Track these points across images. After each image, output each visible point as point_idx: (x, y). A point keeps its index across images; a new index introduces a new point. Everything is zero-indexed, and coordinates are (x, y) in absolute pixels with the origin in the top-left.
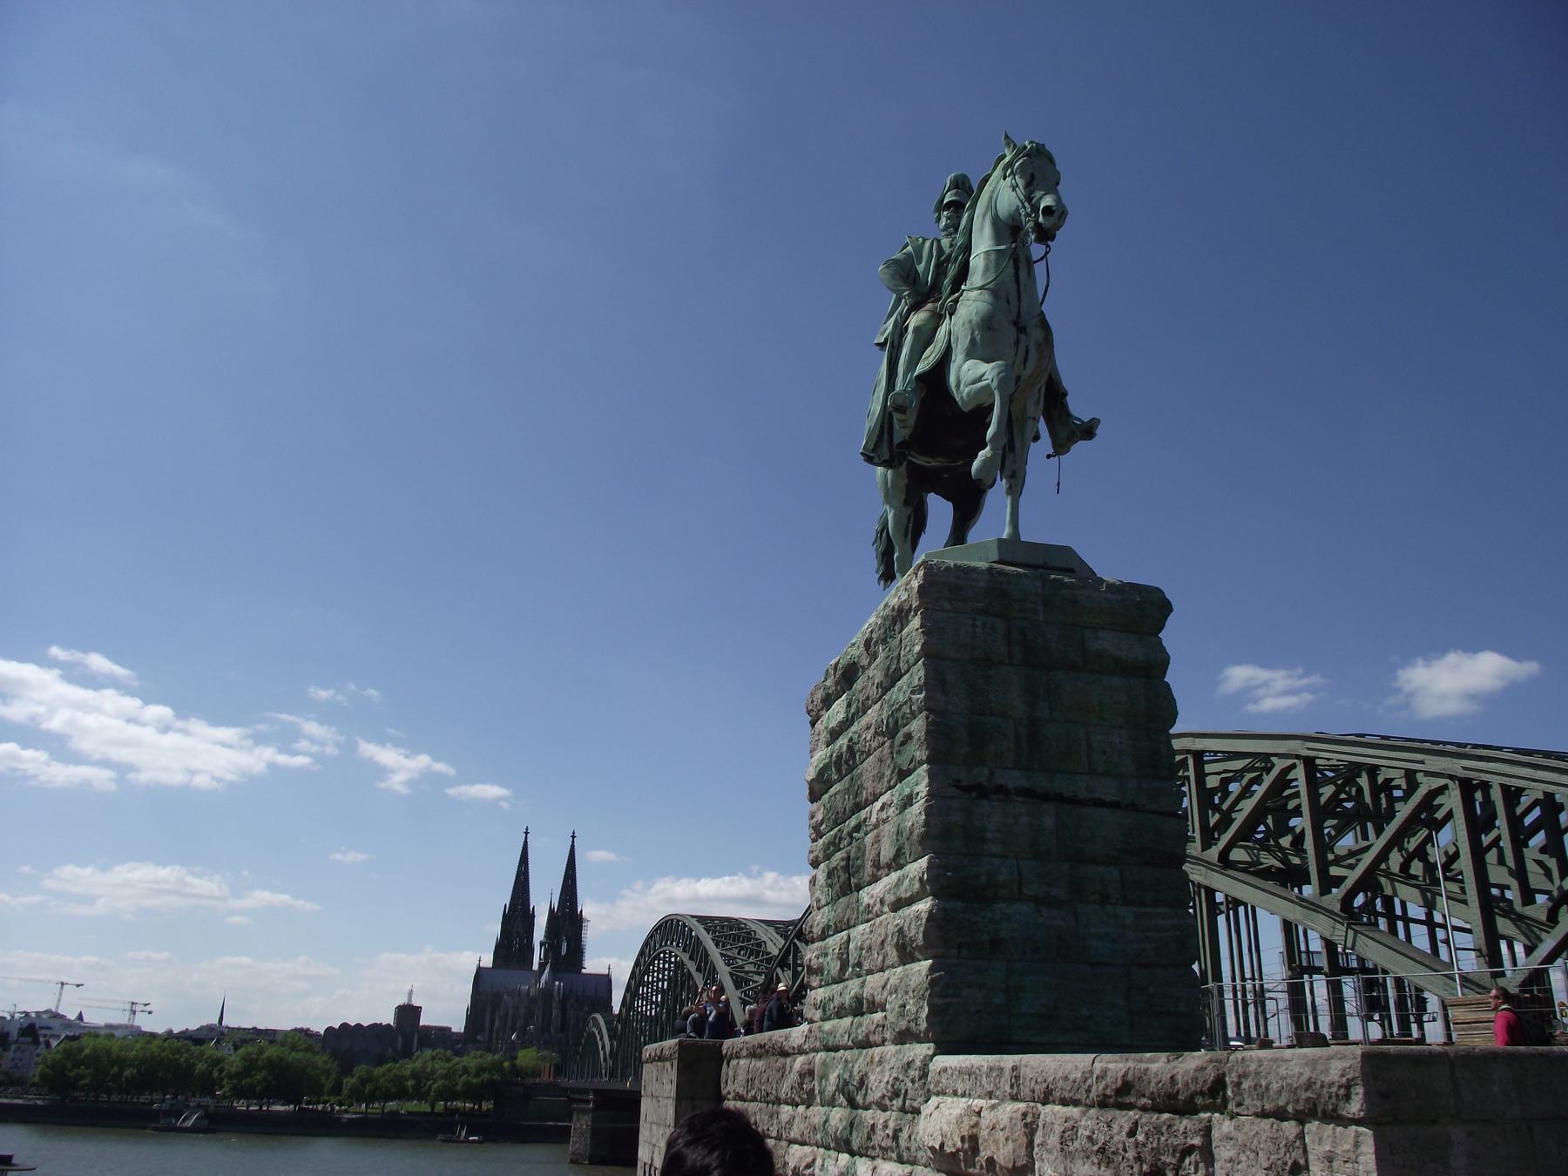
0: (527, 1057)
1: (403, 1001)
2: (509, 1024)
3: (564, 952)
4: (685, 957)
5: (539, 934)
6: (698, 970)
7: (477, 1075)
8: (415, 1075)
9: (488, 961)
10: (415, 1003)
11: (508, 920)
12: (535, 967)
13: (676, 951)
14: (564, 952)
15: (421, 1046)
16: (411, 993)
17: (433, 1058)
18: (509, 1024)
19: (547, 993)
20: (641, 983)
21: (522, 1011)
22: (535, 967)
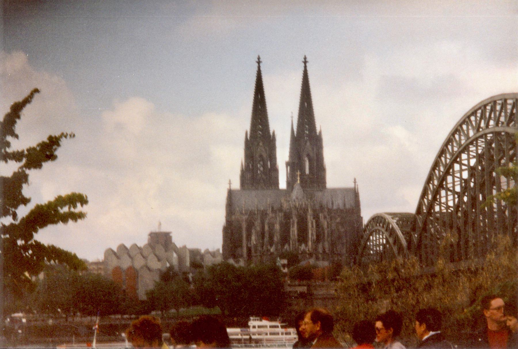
3: (307, 171)
5: (283, 154)
9: (236, 185)
21: (277, 227)
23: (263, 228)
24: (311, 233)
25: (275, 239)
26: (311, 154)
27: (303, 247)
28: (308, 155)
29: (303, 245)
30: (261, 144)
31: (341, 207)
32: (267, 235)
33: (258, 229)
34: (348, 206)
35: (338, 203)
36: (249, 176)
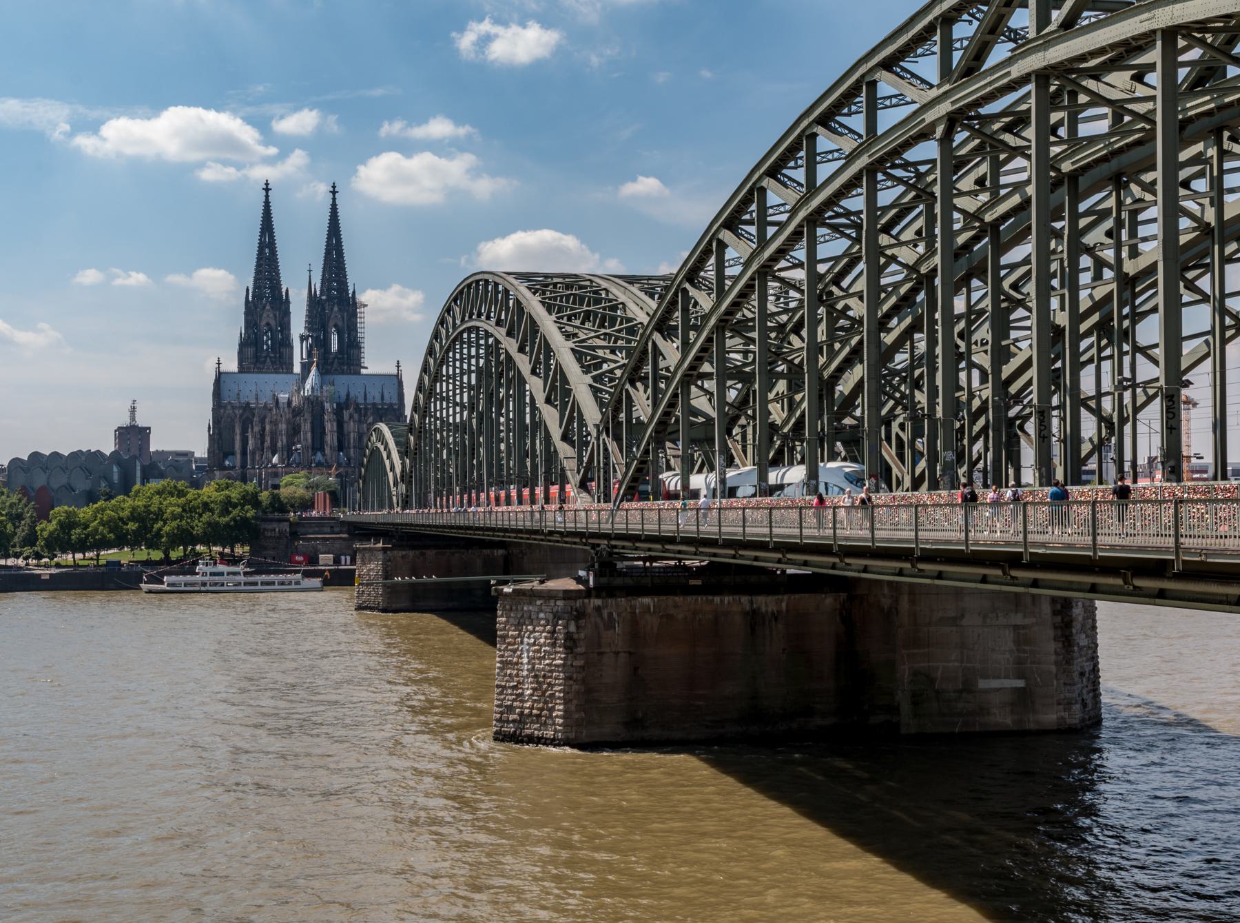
0: (293, 486)
1: (125, 421)
3: (334, 347)
4: (500, 333)
6: (521, 350)
7: (225, 512)
8: (134, 517)
10: (141, 422)
11: (252, 310)
12: (297, 369)
13: (490, 326)
14: (334, 347)
15: (145, 479)
16: (133, 411)
17: (159, 493)
19: (314, 404)
20: (436, 378)
21: (283, 426)
22: (297, 369)
23: (263, 429)
24: (330, 438)
25: (279, 444)
26: (340, 324)
27: (319, 456)
28: (335, 326)
29: (319, 454)
30: (268, 307)
31: (378, 400)
32: (268, 439)
33: (257, 429)
34: (387, 400)
35: (374, 395)
36: (250, 351)
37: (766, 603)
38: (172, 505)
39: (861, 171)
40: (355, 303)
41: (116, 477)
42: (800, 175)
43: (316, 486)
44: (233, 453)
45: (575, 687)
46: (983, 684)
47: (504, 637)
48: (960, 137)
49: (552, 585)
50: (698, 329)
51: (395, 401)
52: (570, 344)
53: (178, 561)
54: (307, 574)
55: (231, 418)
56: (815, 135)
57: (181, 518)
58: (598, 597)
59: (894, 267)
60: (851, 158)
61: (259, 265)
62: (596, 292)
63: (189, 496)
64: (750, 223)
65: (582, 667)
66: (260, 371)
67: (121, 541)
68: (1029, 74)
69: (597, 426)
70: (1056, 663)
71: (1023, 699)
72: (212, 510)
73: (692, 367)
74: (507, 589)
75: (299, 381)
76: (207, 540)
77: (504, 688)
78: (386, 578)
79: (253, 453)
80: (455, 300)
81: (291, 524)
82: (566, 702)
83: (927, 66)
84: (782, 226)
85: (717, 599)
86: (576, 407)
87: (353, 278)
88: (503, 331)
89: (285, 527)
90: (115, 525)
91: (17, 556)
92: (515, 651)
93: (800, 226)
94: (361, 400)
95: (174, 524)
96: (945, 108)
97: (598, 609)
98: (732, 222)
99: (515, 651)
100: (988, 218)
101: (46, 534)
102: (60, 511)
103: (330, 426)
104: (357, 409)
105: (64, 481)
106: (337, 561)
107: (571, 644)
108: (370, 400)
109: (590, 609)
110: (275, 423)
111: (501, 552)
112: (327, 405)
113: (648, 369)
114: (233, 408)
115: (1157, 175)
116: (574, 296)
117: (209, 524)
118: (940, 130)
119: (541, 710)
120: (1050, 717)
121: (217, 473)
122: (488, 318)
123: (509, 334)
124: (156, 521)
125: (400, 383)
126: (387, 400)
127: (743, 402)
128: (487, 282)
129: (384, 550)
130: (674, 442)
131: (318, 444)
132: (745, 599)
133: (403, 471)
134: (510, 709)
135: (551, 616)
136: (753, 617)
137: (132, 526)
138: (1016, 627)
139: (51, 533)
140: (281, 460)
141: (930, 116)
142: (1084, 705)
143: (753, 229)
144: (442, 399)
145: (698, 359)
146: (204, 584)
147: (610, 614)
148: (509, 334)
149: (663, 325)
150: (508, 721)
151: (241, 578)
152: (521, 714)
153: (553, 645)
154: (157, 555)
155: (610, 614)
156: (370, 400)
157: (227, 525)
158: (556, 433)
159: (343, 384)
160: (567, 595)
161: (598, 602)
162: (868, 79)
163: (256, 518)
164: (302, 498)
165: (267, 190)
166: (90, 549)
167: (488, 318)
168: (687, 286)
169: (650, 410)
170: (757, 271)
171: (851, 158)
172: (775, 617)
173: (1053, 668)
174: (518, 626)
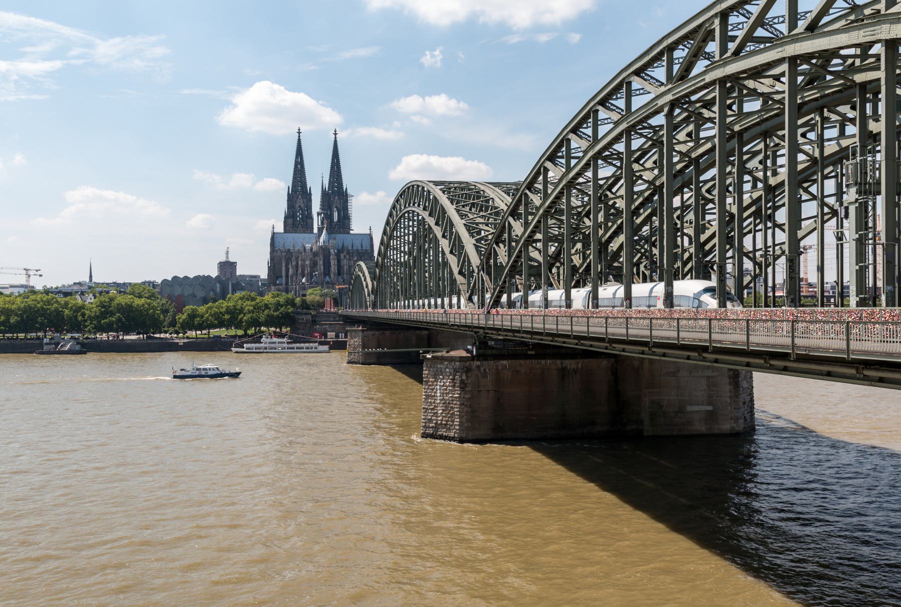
0: (313, 295)
1: (223, 259)
2: (300, 271)
3: (336, 219)
4: (425, 215)
6: (437, 224)
7: (276, 310)
8: (228, 311)
10: (231, 260)
11: (291, 199)
12: (316, 231)
13: (419, 210)
14: (336, 219)
15: (234, 291)
16: (227, 253)
17: (241, 299)
18: (300, 271)
19: (325, 250)
20: (391, 237)
21: (307, 263)
22: (316, 231)
24: (334, 268)
31: (359, 248)
33: (294, 263)
34: (364, 248)
35: (357, 245)
36: (290, 221)
37: (570, 364)
38: (248, 306)
39: (622, 131)
40: (347, 194)
41: (218, 290)
42: (589, 131)
43: (326, 295)
44: (281, 277)
45: (466, 409)
46: (689, 408)
47: (427, 382)
48: (677, 111)
49: (453, 353)
50: (534, 214)
51: (368, 248)
52: (463, 221)
53: (252, 336)
54: (321, 343)
55: (281, 258)
56: (598, 110)
57: (253, 312)
58: (478, 360)
59: (640, 181)
60: (617, 124)
61: (295, 174)
62: (478, 192)
63: (258, 301)
64: (562, 157)
65: (470, 398)
66: (296, 232)
67: (221, 325)
68: (715, 80)
69: (478, 267)
70: (730, 397)
71: (711, 416)
72: (269, 308)
73: (530, 236)
74: (429, 356)
75: (317, 238)
76: (268, 324)
77: (427, 409)
78: (364, 347)
79: (292, 277)
80: (401, 196)
81: (313, 316)
82: (461, 417)
83: (659, 72)
84: (580, 159)
85: (543, 362)
86: (466, 255)
87: (348, 182)
88: (427, 213)
89: (309, 317)
90: (217, 316)
91: (166, 332)
92: (433, 389)
93: (589, 160)
94: (350, 248)
95: (249, 315)
96: (669, 97)
97: (478, 367)
98: (552, 157)
99: (433, 389)
100: (693, 155)
101: (181, 321)
102: (189, 308)
103: (333, 262)
104: (348, 253)
105: (191, 292)
106: (337, 336)
107: (463, 386)
108: (355, 248)
109: (474, 367)
110: (304, 260)
111: (426, 332)
112: (332, 251)
113: (506, 235)
114: (281, 252)
115: (786, 132)
116: (465, 194)
117: (268, 316)
118: (666, 109)
119: (447, 421)
120: (726, 426)
121: (273, 287)
122: (419, 206)
123: (430, 215)
124: (239, 314)
125: (372, 239)
126: (364, 248)
127: (558, 254)
128: (418, 186)
129: (363, 331)
130: (521, 276)
131: (327, 272)
132: (558, 362)
133: (373, 288)
134: (430, 421)
135: (452, 371)
136: (563, 372)
137: (227, 317)
138: (708, 377)
139: (184, 320)
140: (307, 281)
141: (660, 102)
142: (745, 420)
143: (563, 161)
144: (394, 249)
145: (533, 232)
146: (266, 348)
147: (485, 370)
148: (430, 215)
149: (514, 213)
150: (429, 427)
151: (286, 345)
152: (436, 423)
153: (454, 386)
154: (240, 332)
155: (485, 370)
156: (355, 248)
157: (278, 316)
158: (456, 270)
159: (340, 238)
160: (461, 359)
161: (478, 363)
162: (627, 80)
163: (293, 312)
164: (318, 302)
165: (299, 133)
166: (204, 329)
167: (419, 206)
168: (527, 192)
169: (506, 259)
170: (565, 185)
171: (617, 124)
172: (575, 371)
173: (729, 400)
174: (435, 377)
